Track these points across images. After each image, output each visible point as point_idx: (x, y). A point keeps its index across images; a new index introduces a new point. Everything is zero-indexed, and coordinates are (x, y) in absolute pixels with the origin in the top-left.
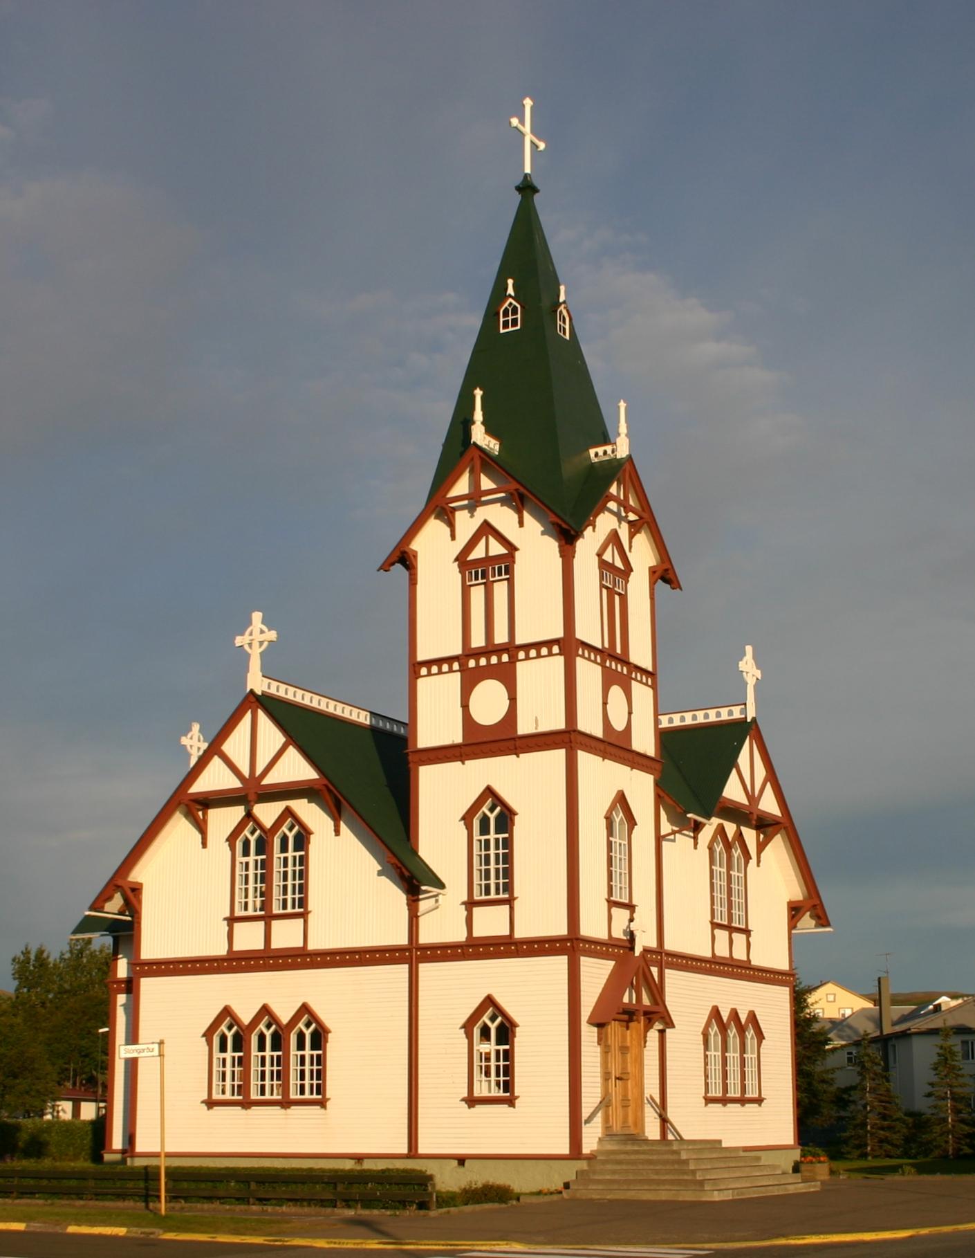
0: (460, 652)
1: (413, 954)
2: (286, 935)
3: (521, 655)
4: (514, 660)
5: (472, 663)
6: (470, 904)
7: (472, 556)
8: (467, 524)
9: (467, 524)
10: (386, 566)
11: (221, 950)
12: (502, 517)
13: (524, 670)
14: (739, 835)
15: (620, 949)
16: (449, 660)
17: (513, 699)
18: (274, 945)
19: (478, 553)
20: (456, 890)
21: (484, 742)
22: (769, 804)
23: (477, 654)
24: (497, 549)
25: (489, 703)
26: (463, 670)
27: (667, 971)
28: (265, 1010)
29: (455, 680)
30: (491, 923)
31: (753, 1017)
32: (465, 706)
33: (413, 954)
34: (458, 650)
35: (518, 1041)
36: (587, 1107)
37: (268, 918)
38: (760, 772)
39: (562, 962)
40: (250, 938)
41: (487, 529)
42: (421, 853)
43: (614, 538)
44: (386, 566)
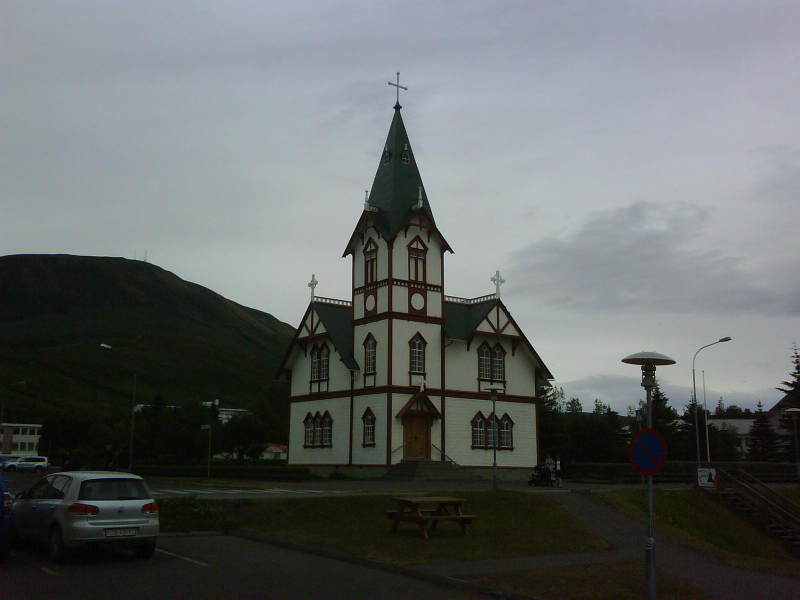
0: (363, 285)
1: (352, 393)
2: (324, 388)
4: (377, 288)
5: (367, 289)
6: (365, 375)
10: (344, 256)
11: (307, 392)
14: (498, 345)
15: (411, 389)
17: (376, 301)
18: (321, 391)
19: (369, 250)
20: (362, 371)
22: (510, 331)
24: (373, 248)
27: (446, 398)
28: (318, 413)
30: (370, 382)
31: (506, 416)
32: (365, 304)
33: (352, 393)
35: (376, 423)
36: (394, 446)
37: (319, 382)
38: (504, 320)
40: (315, 389)
41: (371, 241)
42: (355, 358)
43: (418, 239)
44: (344, 256)
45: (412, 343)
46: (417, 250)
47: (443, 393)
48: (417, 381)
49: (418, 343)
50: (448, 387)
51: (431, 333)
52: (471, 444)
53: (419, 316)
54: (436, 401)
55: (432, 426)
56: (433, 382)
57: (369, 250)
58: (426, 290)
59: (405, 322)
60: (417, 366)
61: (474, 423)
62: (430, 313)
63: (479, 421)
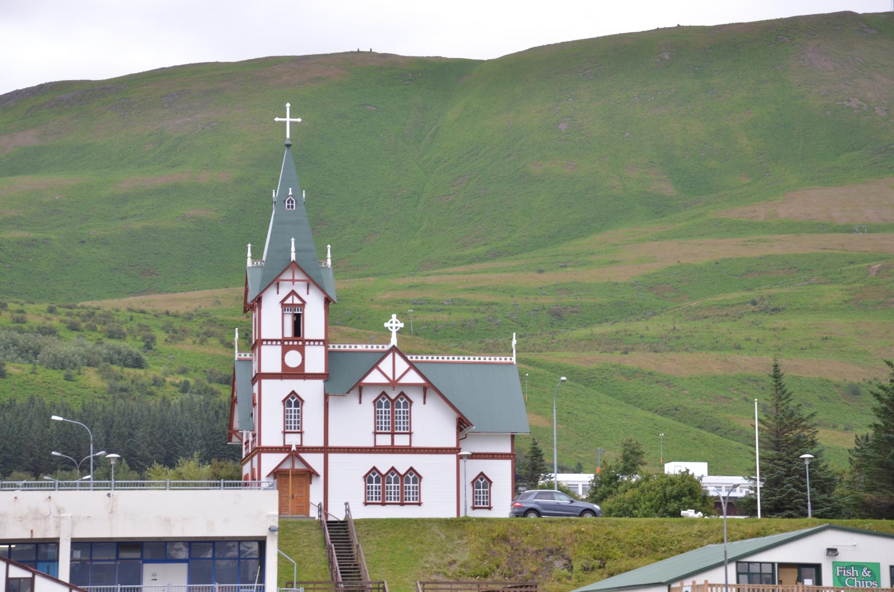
3: (307, 343)
7: (286, 302)
8: (285, 290)
9: (285, 290)
12: (301, 290)
13: (308, 349)
16: (277, 340)
17: (303, 359)
19: (289, 301)
21: (288, 373)
23: (288, 340)
25: (293, 359)
26: (282, 344)
34: (280, 337)
41: (293, 293)
45: (286, 402)
46: (293, 305)
48: (293, 440)
49: (293, 401)
50: (331, 444)
52: (363, 500)
53: (298, 373)
54: (315, 461)
55: (311, 483)
56: (313, 438)
57: (289, 301)
58: (304, 345)
59: (279, 381)
61: (368, 478)
62: (308, 370)
63: (372, 476)
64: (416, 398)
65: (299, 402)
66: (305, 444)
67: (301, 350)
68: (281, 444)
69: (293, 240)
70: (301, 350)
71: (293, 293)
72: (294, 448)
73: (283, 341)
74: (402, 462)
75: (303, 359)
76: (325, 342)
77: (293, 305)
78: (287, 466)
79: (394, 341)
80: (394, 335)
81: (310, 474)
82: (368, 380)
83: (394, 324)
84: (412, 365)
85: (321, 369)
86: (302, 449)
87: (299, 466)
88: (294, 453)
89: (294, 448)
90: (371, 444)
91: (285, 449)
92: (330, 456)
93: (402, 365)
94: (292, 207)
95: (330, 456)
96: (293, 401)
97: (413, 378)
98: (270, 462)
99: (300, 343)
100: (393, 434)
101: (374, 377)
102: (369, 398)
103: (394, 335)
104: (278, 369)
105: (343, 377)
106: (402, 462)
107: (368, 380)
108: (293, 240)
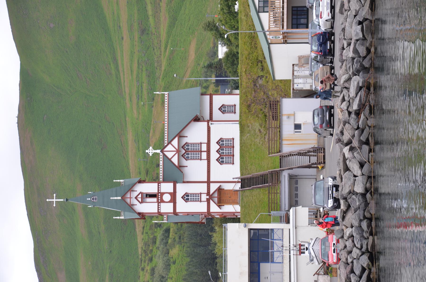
3: (159, 191)
7: (140, 201)
8: (135, 202)
9: (135, 202)
12: (135, 194)
13: (162, 191)
16: (158, 205)
17: (167, 193)
19: (140, 200)
21: (173, 200)
24: (140, 196)
25: (167, 197)
26: (160, 203)
29: (162, 204)
34: (157, 204)
39: (211, 184)
41: (136, 198)
45: (187, 200)
47: (209, 182)
48: (204, 197)
49: (186, 197)
50: (206, 180)
51: (182, 189)
52: (232, 165)
53: (173, 195)
54: (214, 187)
55: (224, 189)
56: (203, 188)
58: (160, 193)
60: (196, 197)
61: (221, 163)
62: (172, 191)
64: (184, 141)
65: (187, 195)
66: (206, 192)
67: (163, 194)
68: (206, 203)
69: (111, 198)
70: (163, 194)
71: (136, 198)
72: (208, 197)
73: (158, 202)
74: (214, 147)
75: (167, 193)
76: (159, 183)
77: (142, 198)
78: (216, 200)
79: (158, 151)
80: (156, 151)
81: (219, 190)
82: (176, 163)
83: (151, 151)
84: (169, 143)
85: (172, 184)
86: (208, 193)
87: (216, 195)
88: (210, 197)
89: (208, 197)
90: (206, 162)
91: (208, 201)
92: (211, 180)
93: (169, 148)
94: (96, 198)
95: (211, 180)
96: (186, 197)
97: (175, 142)
98: (214, 208)
99: (159, 194)
100: (201, 151)
101: (175, 160)
102: (185, 162)
103: (156, 151)
104: (172, 204)
105: (175, 175)
106: (214, 147)
107: (176, 163)
108: (111, 198)
